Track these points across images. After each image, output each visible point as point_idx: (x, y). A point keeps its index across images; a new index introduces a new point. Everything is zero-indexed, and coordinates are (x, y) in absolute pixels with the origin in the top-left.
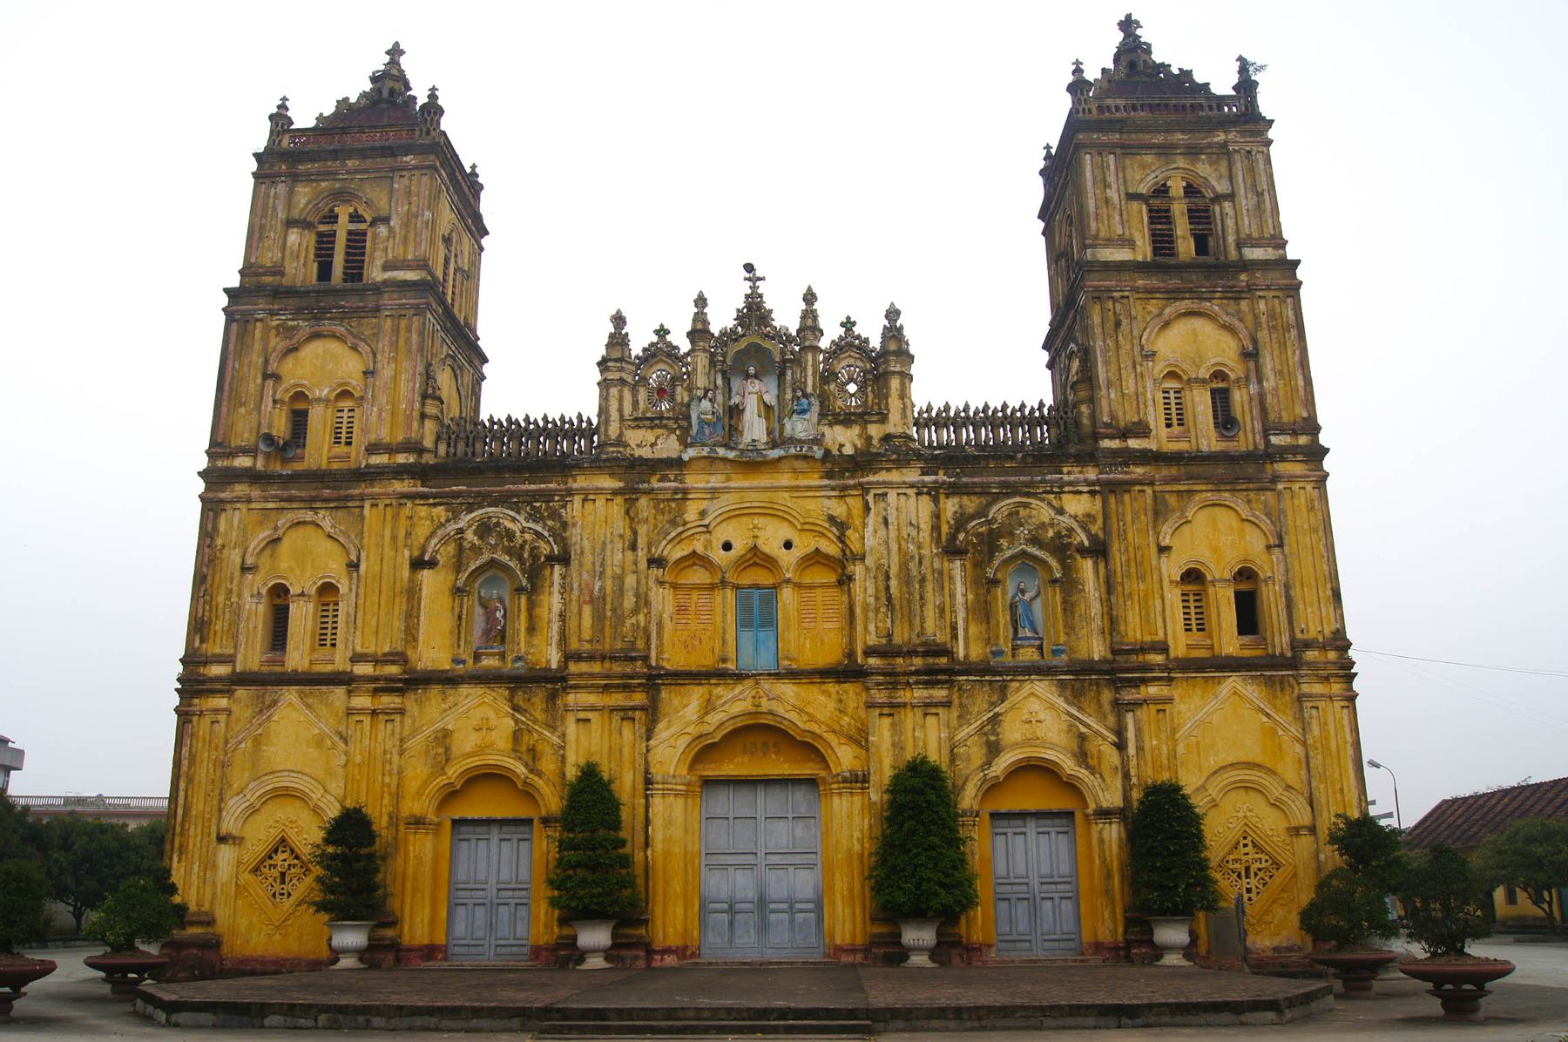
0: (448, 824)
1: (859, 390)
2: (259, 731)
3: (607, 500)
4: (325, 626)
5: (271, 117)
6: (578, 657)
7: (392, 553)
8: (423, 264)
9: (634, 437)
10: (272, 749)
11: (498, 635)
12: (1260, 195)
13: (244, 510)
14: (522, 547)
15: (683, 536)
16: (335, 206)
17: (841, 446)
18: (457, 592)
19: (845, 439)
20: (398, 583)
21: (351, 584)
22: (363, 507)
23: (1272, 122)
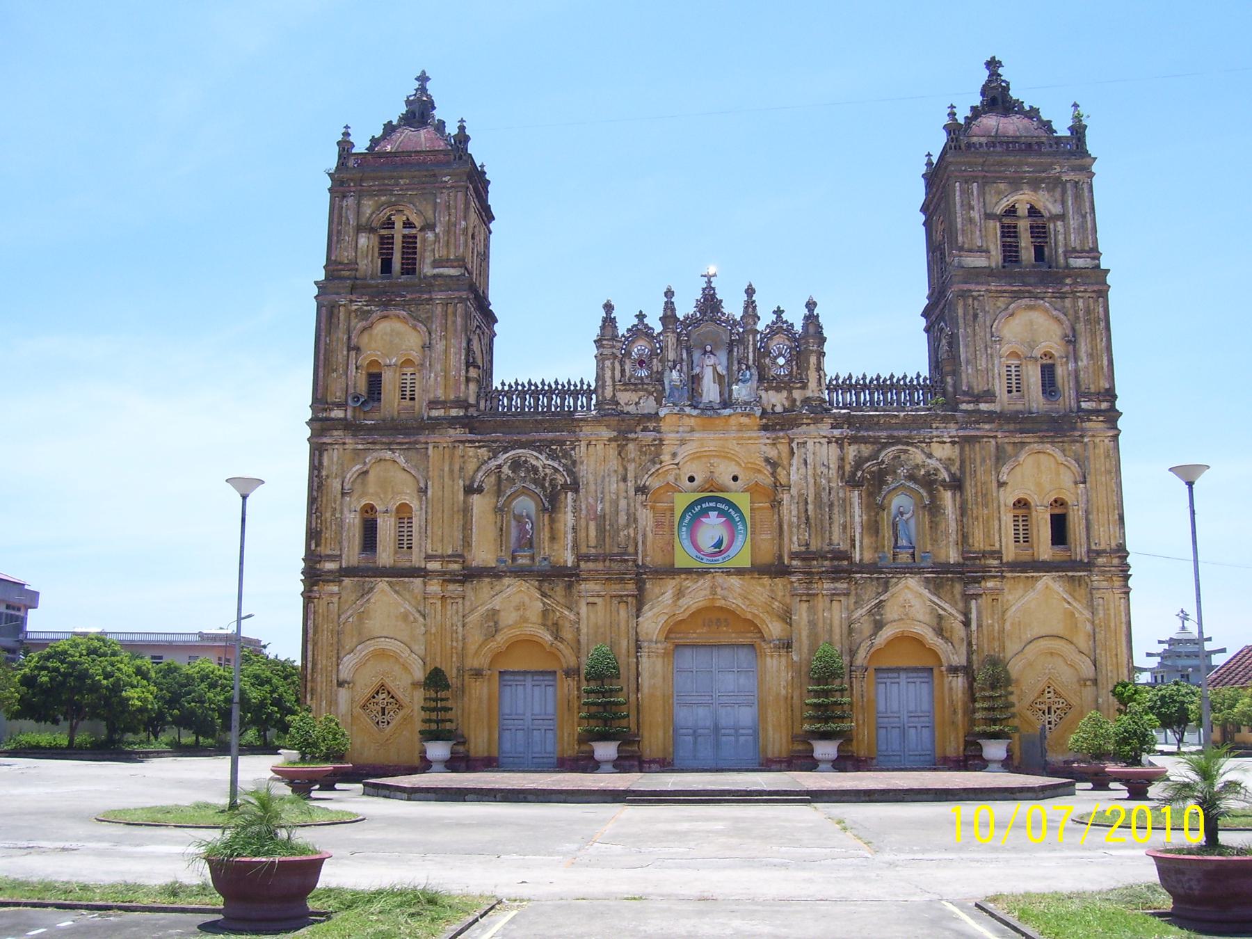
0: (497, 674)
1: (787, 362)
2: (362, 610)
3: (605, 444)
4: (402, 534)
5: (338, 143)
6: (587, 558)
7: (451, 483)
8: (461, 262)
9: (623, 397)
10: (372, 622)
11: (528, 543)
12: (1084, 217)
13: (341, 450)
14: (544, 479)
15: (660, 471)
16: (391, 215)
17: (774, 406)
18: (498, 510)
19: (776, 400)
20: (456, 505)
21: (421, 504)
22: (427, 448)
23: (1095, 159)
